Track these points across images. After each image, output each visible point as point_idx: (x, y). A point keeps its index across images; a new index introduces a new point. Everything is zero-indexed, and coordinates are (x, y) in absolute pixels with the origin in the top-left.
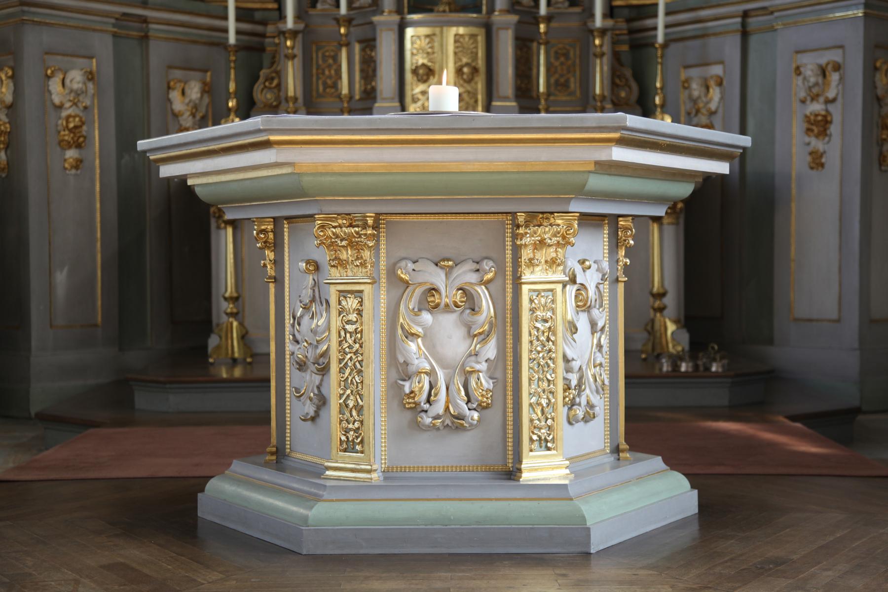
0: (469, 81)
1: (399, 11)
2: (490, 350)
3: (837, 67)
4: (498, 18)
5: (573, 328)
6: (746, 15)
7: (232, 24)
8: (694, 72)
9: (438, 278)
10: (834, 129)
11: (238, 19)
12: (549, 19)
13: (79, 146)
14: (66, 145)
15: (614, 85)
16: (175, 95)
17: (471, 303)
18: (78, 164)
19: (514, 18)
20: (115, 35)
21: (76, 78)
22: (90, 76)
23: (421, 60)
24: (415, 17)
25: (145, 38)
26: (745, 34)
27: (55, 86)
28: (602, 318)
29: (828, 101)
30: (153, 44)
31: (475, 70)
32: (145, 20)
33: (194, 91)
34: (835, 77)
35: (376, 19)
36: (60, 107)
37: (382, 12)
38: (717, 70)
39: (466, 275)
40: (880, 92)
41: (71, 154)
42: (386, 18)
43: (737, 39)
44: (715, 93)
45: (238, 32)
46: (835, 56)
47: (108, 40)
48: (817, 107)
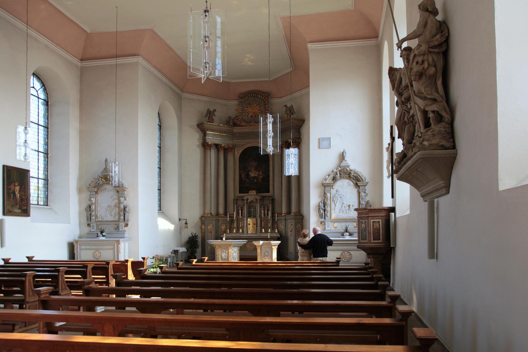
0: (254, 225)
1: (247, 217)
2: (227, 255)
3: (293, 225)
4: (258, 218)
5: (233, 254)
6: (285, 218)
7: (228, 218)
8: (281, 224)
9: (224, 250)
10: (292, 231)
11: (229, 218)
12: (263, 218)
13: (211, 233)
14: (210, 233)
15: (272, 226)
16: (222, 227)
17: (226, 251)
18: (211, 235)
19: (260, 218)
20: (215, 221)
21: (211, 226)
22: (212, 226)
23: (249, 223)
24: (249, 218)
25: (219, 221)
26: (285, 220)
27: (209, 227)
28: (237, 252)
29: (292, 228)
30: (220, 221)
31: (255, 224)
32: (219, 219)
33: (224, 226)
34: (292, 226)
35: (244, 218)
36: (209, 229)
37: (245, 217)
38: (283, 224)
39: (226, 250)
40: (297, 228)
41: (210, 234)
42: (245, 218)
43: (284, 221)
44: (283, 226)
45: (229, 219)
46: (292, 223)
47: (215, 221)
48: (291, 229)
